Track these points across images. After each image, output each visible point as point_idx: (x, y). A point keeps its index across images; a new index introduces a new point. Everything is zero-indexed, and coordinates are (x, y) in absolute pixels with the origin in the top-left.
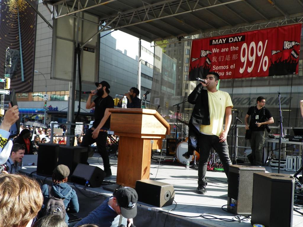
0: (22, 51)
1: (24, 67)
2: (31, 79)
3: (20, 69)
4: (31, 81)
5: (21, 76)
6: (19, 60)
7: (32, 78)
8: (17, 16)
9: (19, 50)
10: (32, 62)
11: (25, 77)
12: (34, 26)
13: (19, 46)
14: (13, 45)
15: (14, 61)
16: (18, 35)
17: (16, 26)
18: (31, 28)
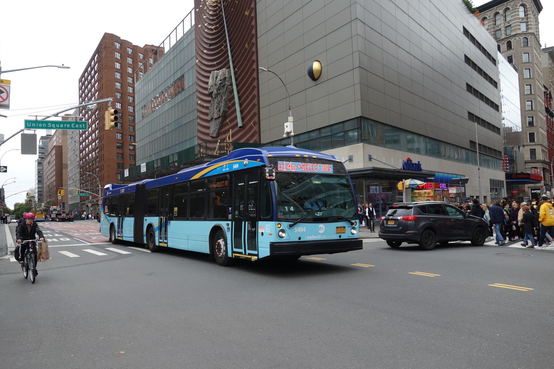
0: (234, 68)
1: (240, 98)
2: (256, 119)
3: (234, 104)
4: (255, 123)
5: (236, 117)
6: (229, 87)
7: (257, 116)
8: (220, 7)
9: (229, 67)
10: (255, 84)
11: (243, 119)
12: (252, 8)
13: (228, 62)
14: (218, 64)
15: (221, 91)
16: (226, 41)
17: (220, 26)
18: (246, 15)
